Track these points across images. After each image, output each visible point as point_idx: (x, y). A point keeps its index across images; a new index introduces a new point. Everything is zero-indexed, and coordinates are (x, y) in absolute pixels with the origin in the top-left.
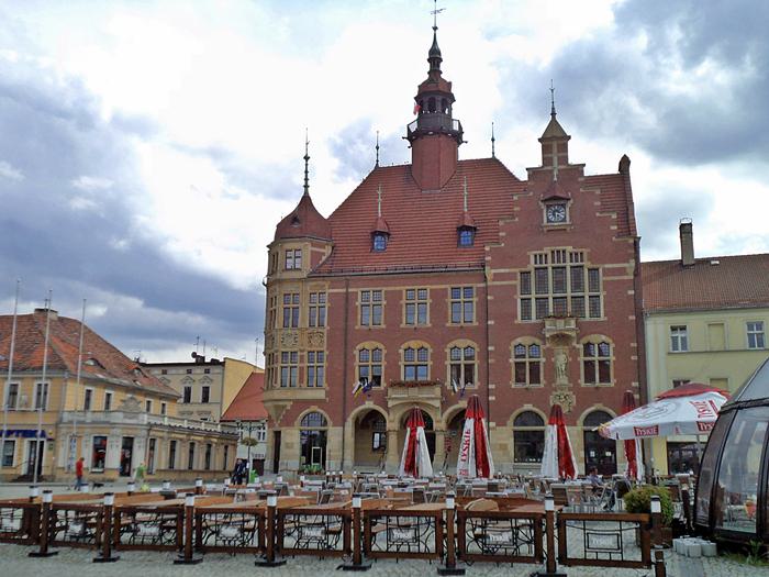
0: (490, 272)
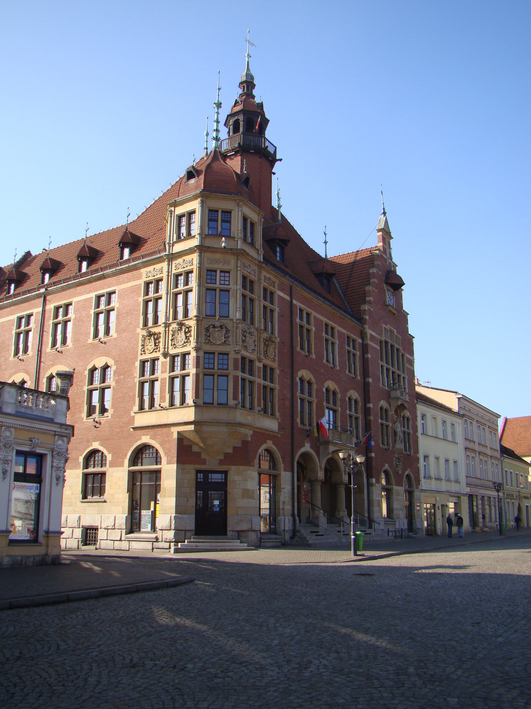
0: (369, 332)
